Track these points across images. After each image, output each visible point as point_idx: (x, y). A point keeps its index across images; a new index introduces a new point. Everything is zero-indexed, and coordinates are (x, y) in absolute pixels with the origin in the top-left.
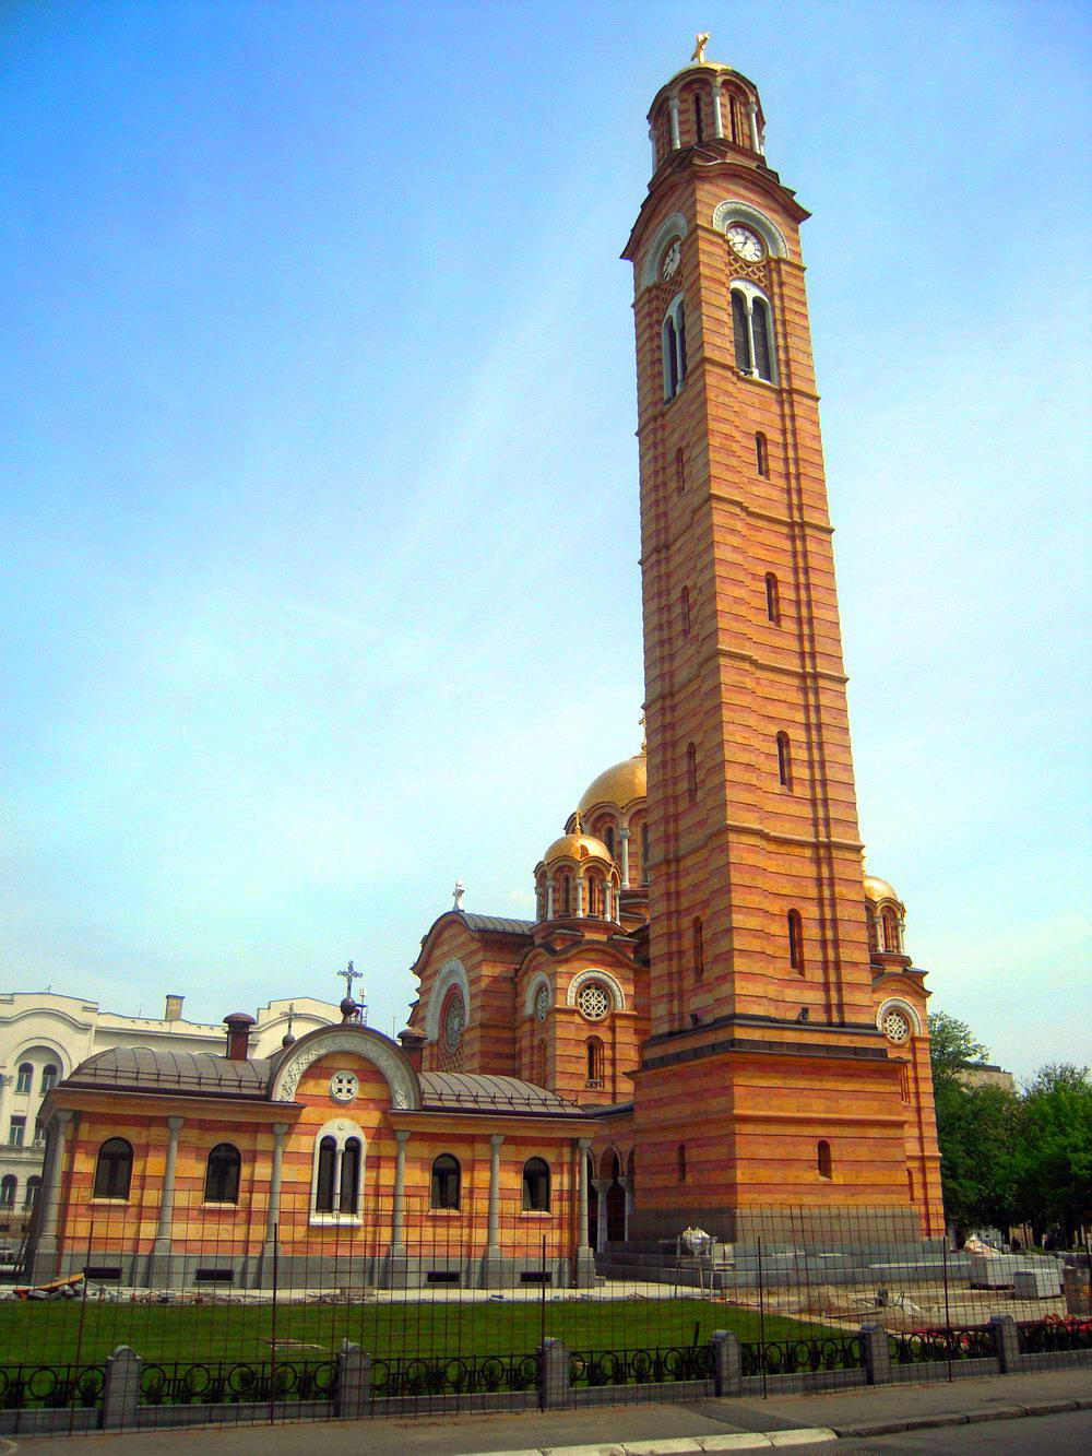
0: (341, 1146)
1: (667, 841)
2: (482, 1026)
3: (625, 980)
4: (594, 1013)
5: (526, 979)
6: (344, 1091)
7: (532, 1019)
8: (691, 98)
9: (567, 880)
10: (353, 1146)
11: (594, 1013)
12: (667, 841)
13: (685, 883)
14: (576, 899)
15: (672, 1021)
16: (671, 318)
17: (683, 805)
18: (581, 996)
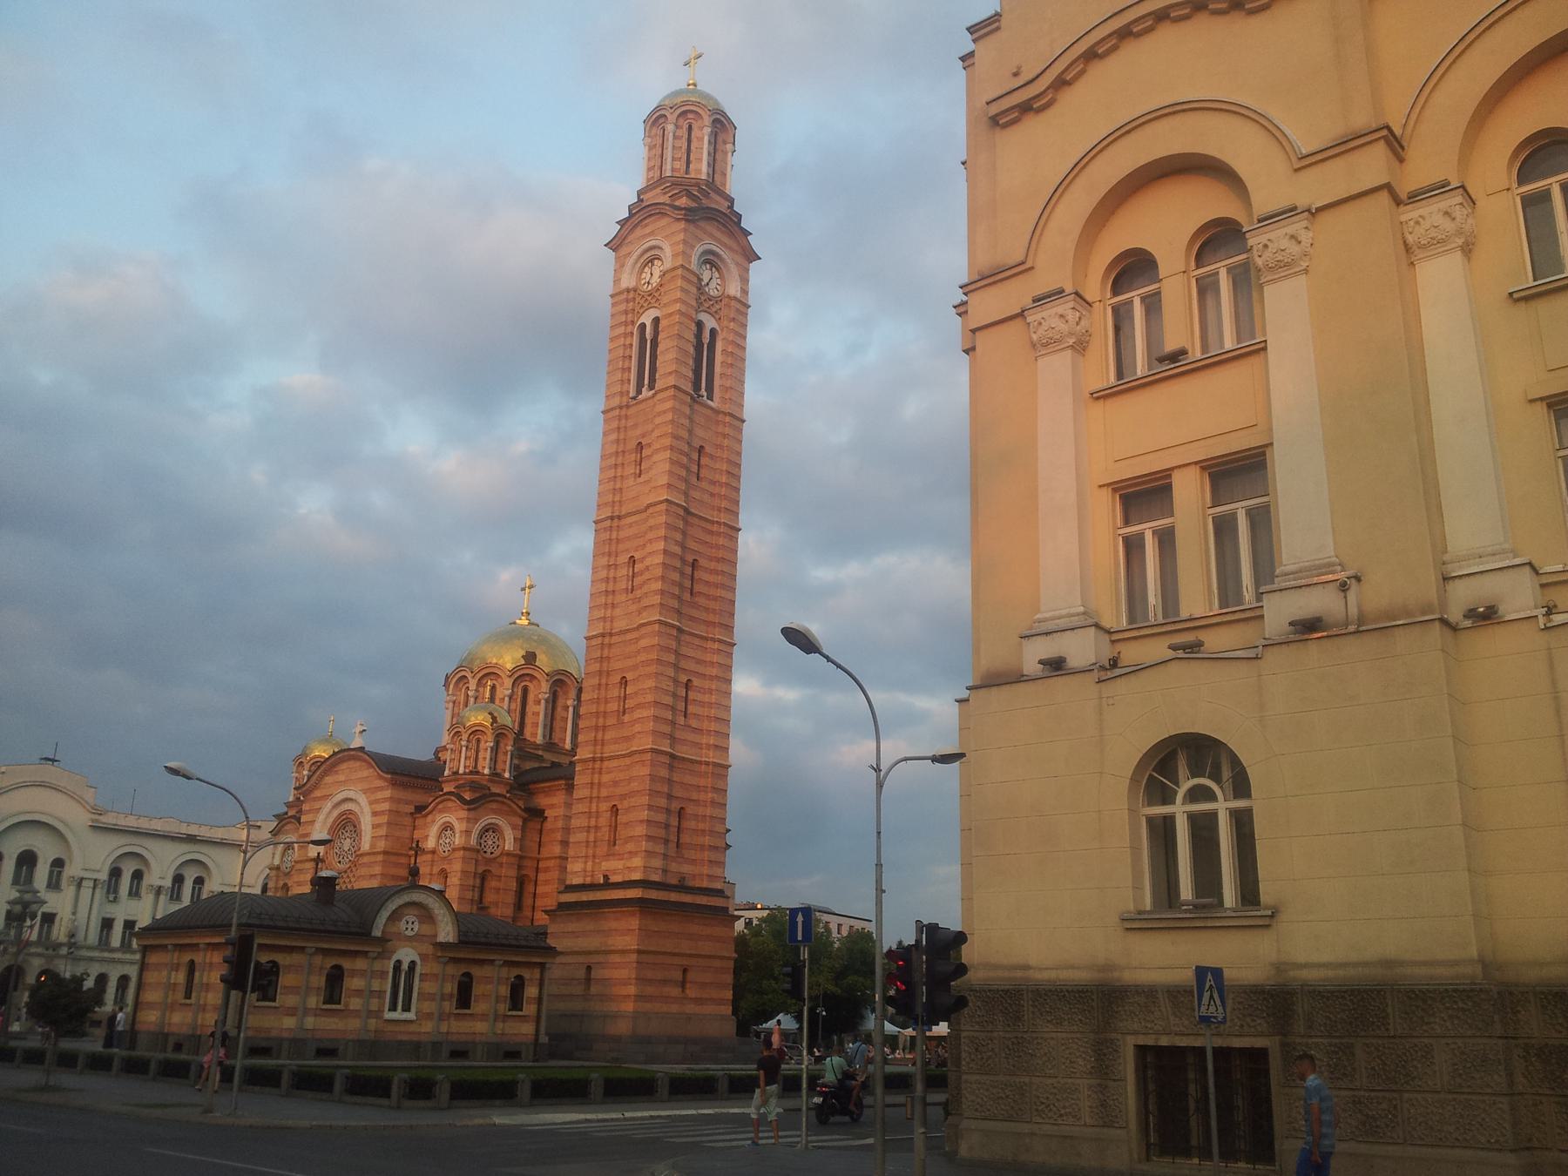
0: (405, 966)
1: (595, 745)
2: (385, 853)
3: (514, 828)
4: (489, 851)
5: (430, 818)
6: (410, 929)
7: (433, 852)
8: (686, 126)
9: (478, 741)
10: (413, 964)
11: (489, 851)
12: (595, 745)
13: (606, 778)
14: (485, 758)
15: (585, 876)
16: (643, 326)
17: (611, 721)
18: (481, 838)
